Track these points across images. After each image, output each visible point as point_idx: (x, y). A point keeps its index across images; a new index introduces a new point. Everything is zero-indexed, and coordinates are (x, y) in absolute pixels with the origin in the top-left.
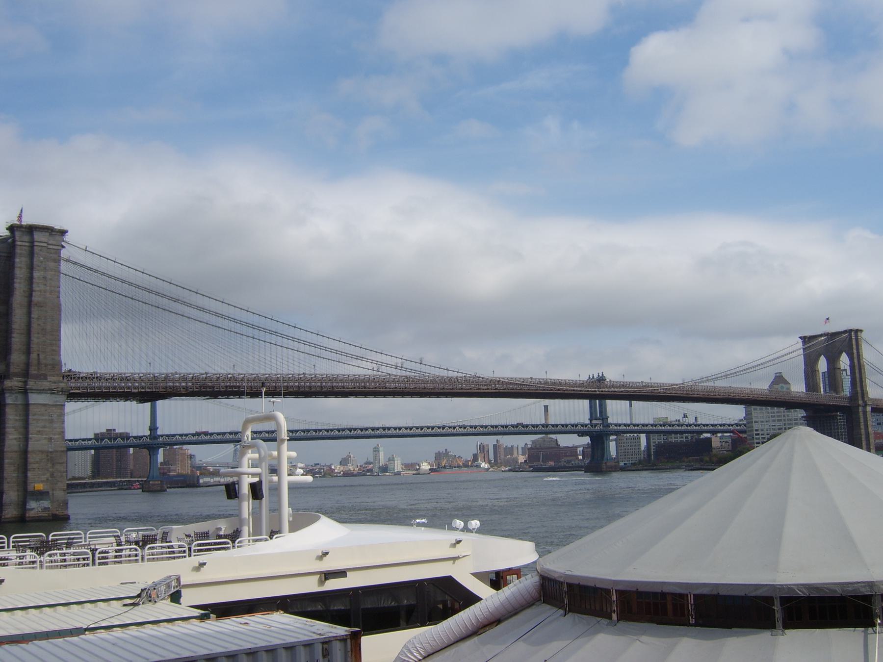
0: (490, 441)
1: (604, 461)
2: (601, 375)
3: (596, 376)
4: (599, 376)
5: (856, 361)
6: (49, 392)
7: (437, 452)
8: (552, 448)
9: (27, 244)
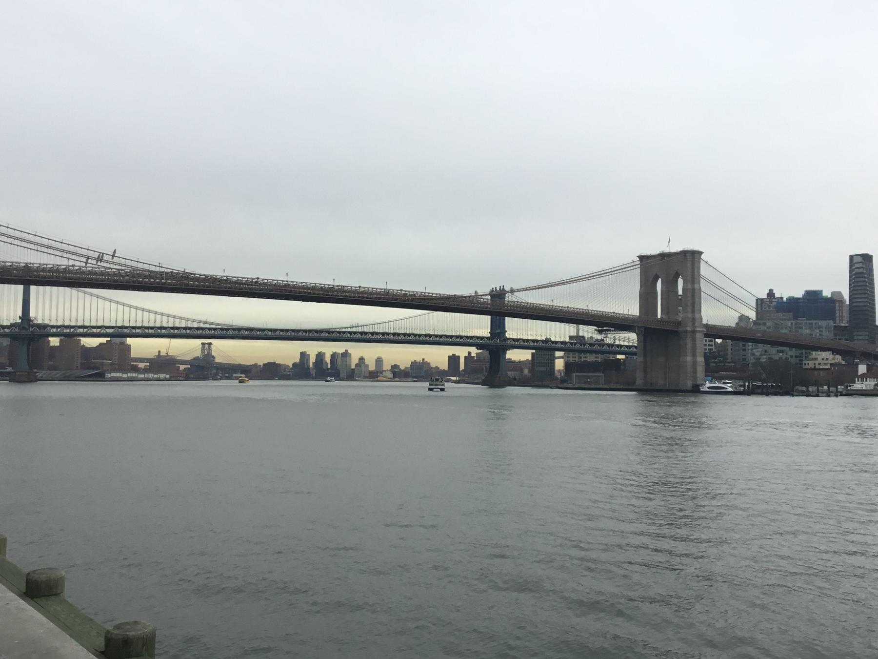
0: (462, 352)
1: (498, 376)
2: (502, 288)
4: (500, 289)
7: (413, 361)
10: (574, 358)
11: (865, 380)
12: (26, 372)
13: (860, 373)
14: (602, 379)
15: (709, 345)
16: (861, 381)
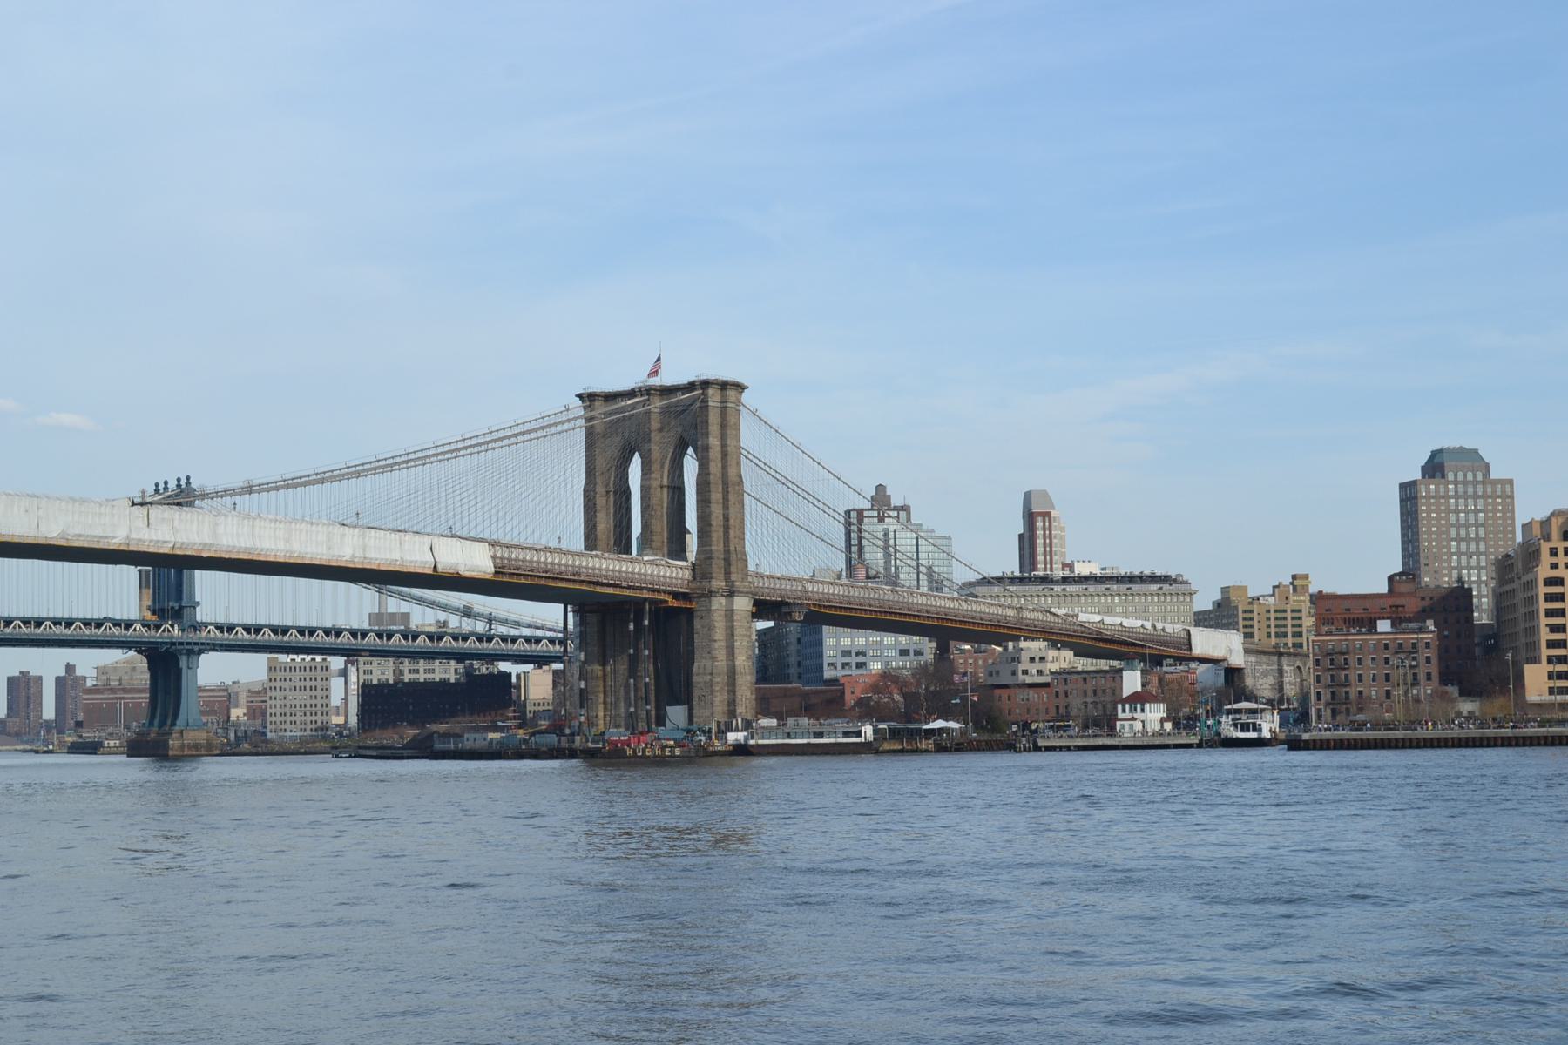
0: (47, 664)
2: (183, 483)
4: (179, 486)
5: (715, 468)
10: (382, 671)
11: (1139, 706)
13: (1126, 692)
16: (1131, 711)
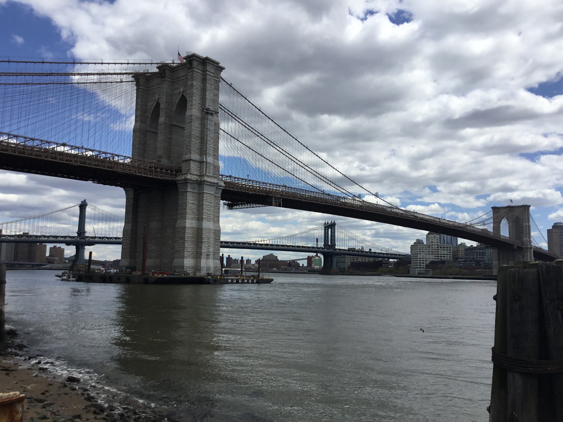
1: (332, 269)
3: (330, 222)
4: (332, 222)
6: (216, 185)
8: (275, 261)
9: (200, 72)
12: (83, 264)
14: (430, 272)
15: (450, 255)
